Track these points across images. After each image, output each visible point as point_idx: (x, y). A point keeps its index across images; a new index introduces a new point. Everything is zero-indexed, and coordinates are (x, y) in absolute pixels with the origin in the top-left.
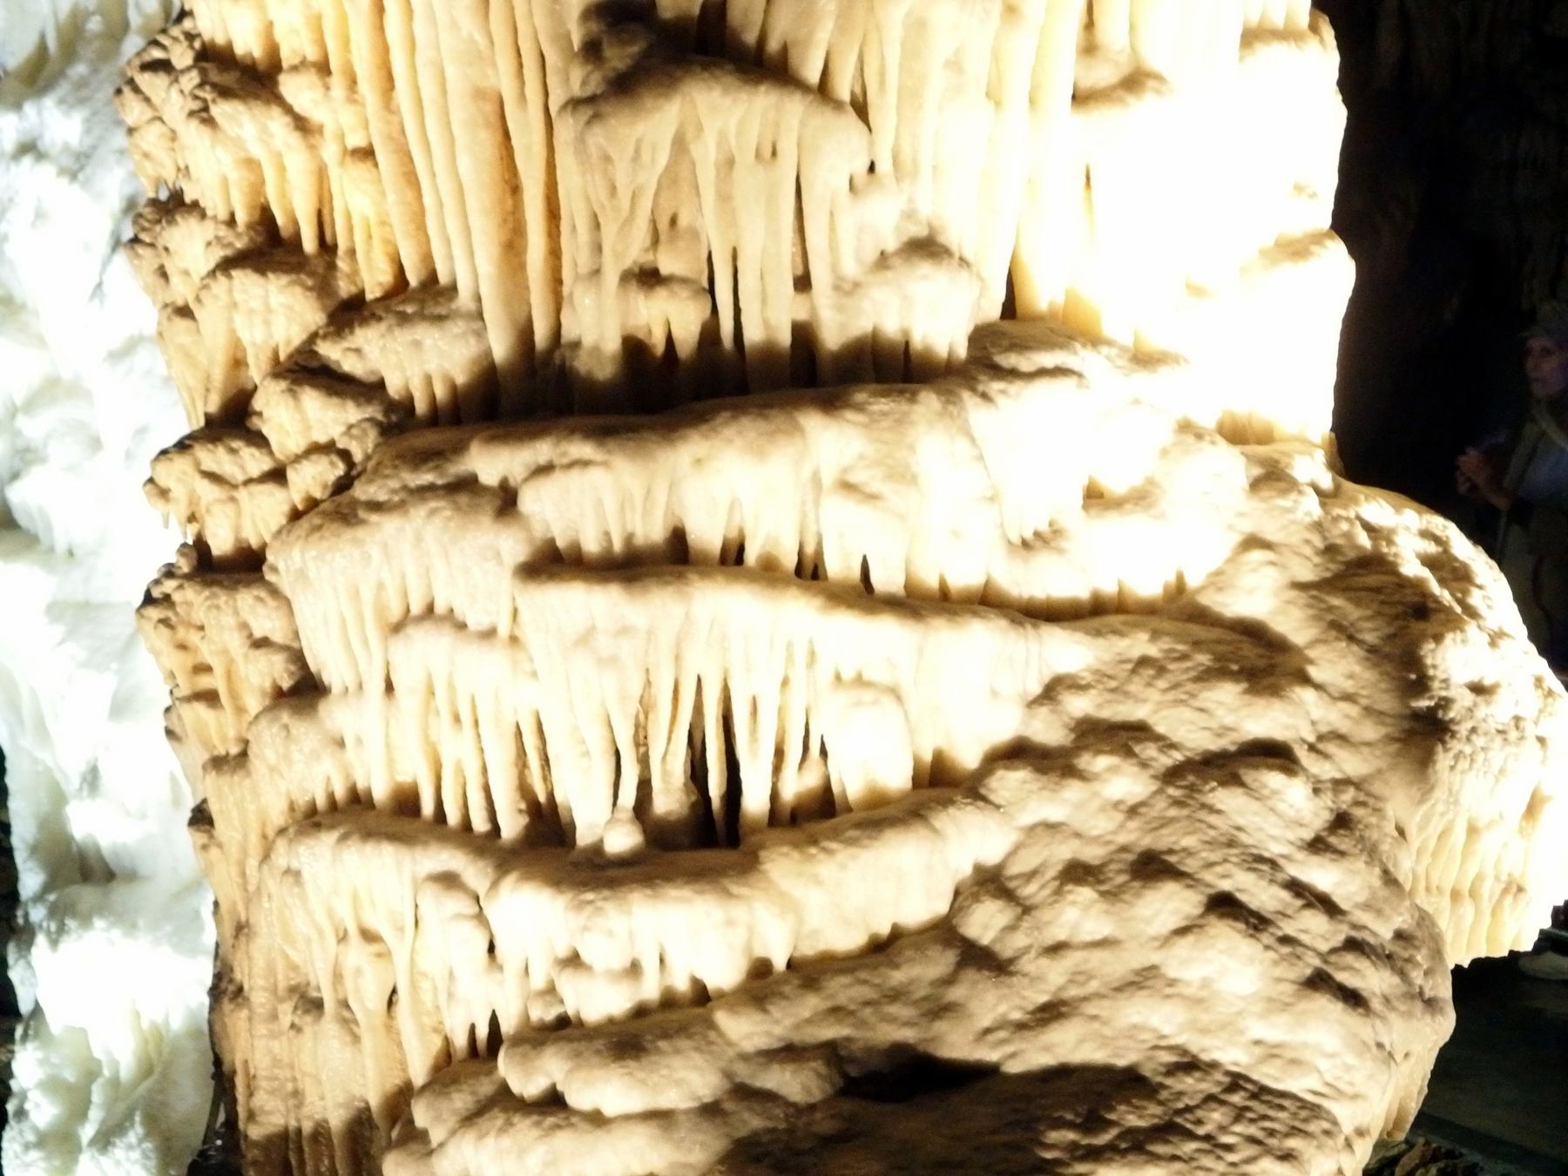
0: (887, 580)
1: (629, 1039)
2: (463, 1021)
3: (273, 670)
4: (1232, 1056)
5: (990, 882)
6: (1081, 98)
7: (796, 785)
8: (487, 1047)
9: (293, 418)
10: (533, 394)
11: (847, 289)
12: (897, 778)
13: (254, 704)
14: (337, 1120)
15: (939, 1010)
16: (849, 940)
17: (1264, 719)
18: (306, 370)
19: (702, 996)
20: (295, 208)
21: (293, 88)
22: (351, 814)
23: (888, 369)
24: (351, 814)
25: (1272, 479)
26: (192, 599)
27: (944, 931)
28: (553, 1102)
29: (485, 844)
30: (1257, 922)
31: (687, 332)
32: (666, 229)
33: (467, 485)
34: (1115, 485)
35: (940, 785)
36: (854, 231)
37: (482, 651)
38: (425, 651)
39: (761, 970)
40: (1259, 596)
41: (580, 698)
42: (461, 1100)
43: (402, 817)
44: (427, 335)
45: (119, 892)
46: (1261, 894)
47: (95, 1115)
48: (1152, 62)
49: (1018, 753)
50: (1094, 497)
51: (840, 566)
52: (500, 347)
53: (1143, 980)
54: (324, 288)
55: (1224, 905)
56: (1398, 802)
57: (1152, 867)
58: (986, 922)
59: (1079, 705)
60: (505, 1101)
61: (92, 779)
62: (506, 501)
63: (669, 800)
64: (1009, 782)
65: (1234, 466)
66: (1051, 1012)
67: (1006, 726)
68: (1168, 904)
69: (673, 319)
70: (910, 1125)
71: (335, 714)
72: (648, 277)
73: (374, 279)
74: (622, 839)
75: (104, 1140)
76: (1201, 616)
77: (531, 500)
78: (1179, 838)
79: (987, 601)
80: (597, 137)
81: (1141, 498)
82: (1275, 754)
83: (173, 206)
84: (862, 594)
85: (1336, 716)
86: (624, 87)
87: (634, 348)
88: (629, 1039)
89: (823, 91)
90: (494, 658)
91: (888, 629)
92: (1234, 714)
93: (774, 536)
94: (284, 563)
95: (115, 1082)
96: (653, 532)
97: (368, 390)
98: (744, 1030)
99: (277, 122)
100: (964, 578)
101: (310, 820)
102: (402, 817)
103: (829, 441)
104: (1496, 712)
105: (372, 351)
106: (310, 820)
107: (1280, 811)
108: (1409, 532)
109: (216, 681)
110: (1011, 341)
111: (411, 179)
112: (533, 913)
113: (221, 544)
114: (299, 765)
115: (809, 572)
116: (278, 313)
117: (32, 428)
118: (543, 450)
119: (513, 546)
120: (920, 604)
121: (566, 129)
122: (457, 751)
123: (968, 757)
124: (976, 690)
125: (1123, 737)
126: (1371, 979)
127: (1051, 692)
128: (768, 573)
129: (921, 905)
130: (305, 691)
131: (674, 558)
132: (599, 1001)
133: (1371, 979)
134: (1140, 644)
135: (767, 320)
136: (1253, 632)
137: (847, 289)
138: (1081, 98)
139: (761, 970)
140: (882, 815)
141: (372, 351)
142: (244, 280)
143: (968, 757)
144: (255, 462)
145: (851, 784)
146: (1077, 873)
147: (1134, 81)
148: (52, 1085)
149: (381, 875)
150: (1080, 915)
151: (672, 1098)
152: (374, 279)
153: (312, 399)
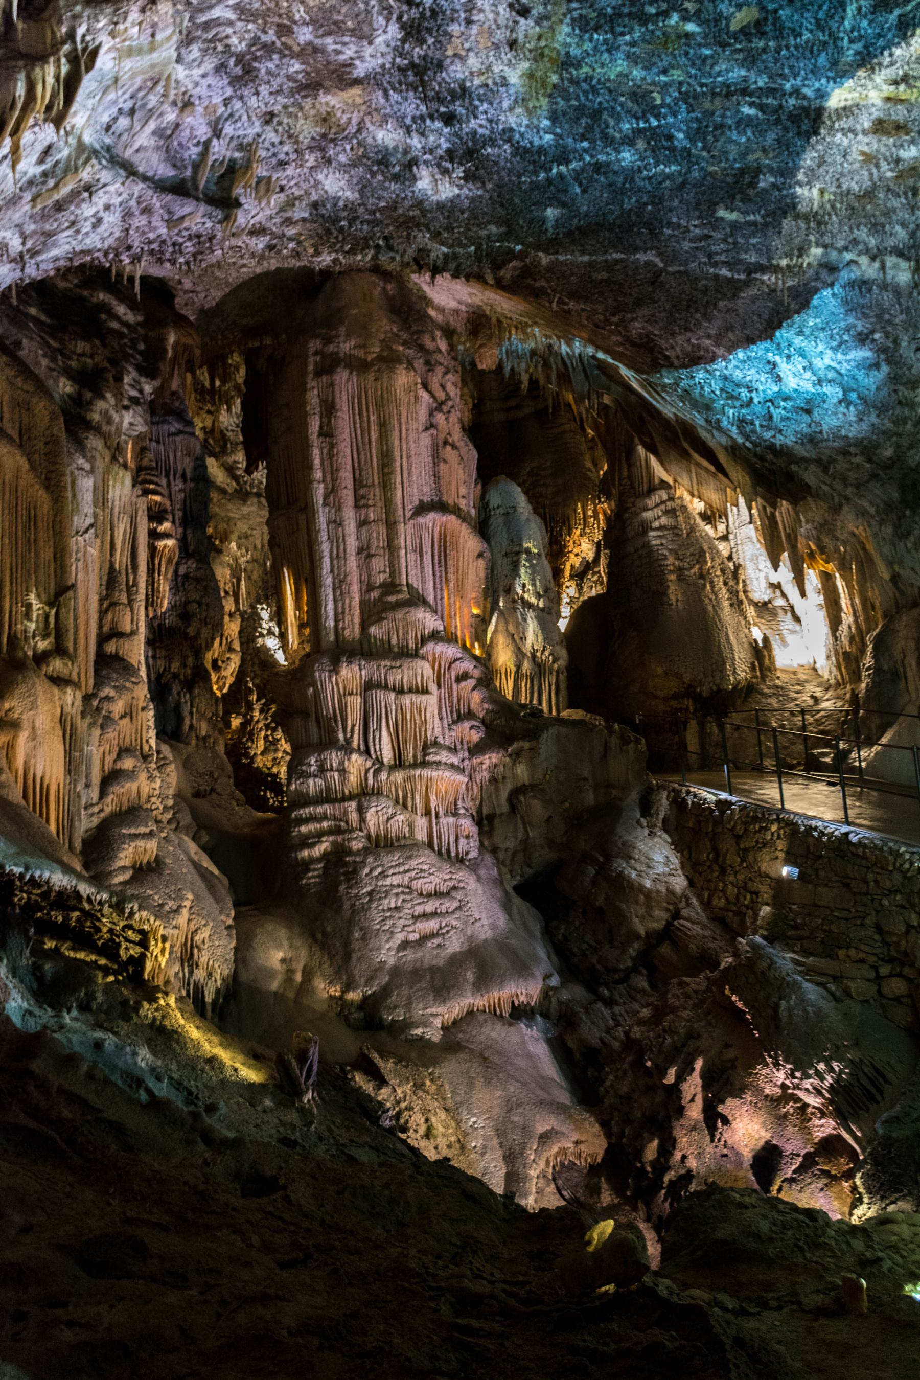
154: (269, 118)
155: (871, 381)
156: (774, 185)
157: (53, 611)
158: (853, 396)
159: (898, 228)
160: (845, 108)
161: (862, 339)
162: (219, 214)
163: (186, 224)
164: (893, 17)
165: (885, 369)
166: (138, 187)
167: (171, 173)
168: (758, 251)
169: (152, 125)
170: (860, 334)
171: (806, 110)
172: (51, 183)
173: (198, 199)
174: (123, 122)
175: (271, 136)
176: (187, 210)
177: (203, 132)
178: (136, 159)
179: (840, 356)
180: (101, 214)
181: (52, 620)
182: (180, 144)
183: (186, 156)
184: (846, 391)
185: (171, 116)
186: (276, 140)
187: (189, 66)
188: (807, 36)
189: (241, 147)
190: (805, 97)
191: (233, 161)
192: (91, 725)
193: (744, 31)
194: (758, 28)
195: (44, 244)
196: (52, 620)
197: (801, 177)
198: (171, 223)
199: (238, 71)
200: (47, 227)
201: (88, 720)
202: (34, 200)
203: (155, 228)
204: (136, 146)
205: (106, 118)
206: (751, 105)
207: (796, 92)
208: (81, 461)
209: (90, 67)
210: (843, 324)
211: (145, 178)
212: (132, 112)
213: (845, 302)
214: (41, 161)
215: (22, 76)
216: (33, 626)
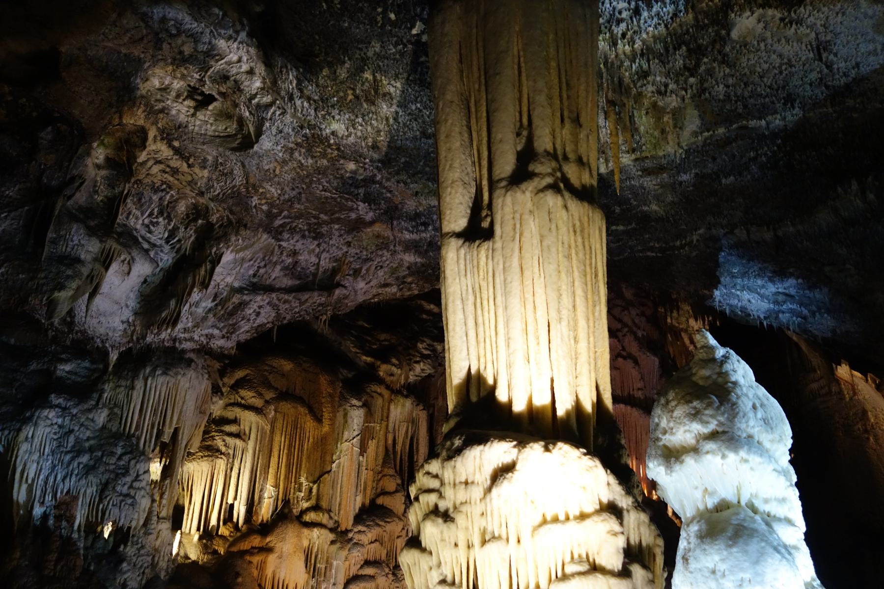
154: (349, 244)
157: (315, 486)
162: (326, 294)
163: (311, 301)
166: (274, 295)
167: (298, 282)
169: (279, 267)
172: (220, 308)
173: (313, 290)
174: (262, 271)
175: (352, 251)
176: (307, 296)
177: (314, 259)
178: (273, 283)
180: (258, 310)
181: (314, 491)
182: (303, 268)
183: (308, 271)
185: (290, 260)
186: (358, 251)
187: (288, 240)
189: (336, 261)
191: (334, 267)
192: (341, 548)
195: (234, 329)
196: (314, 491)
198: (302, 303)
199: (312, 234)
200: (231, 322)
201: (338, 545)
202: (214, 316)
203: (296, 307)
204: (273, 277)
205: (251, 272)
208: (355, 402)
209: (219, 262)
211: (280, 290)
212: (265, 266)
214: (213, 301)
215: (191, 275)
216: (302, 494)
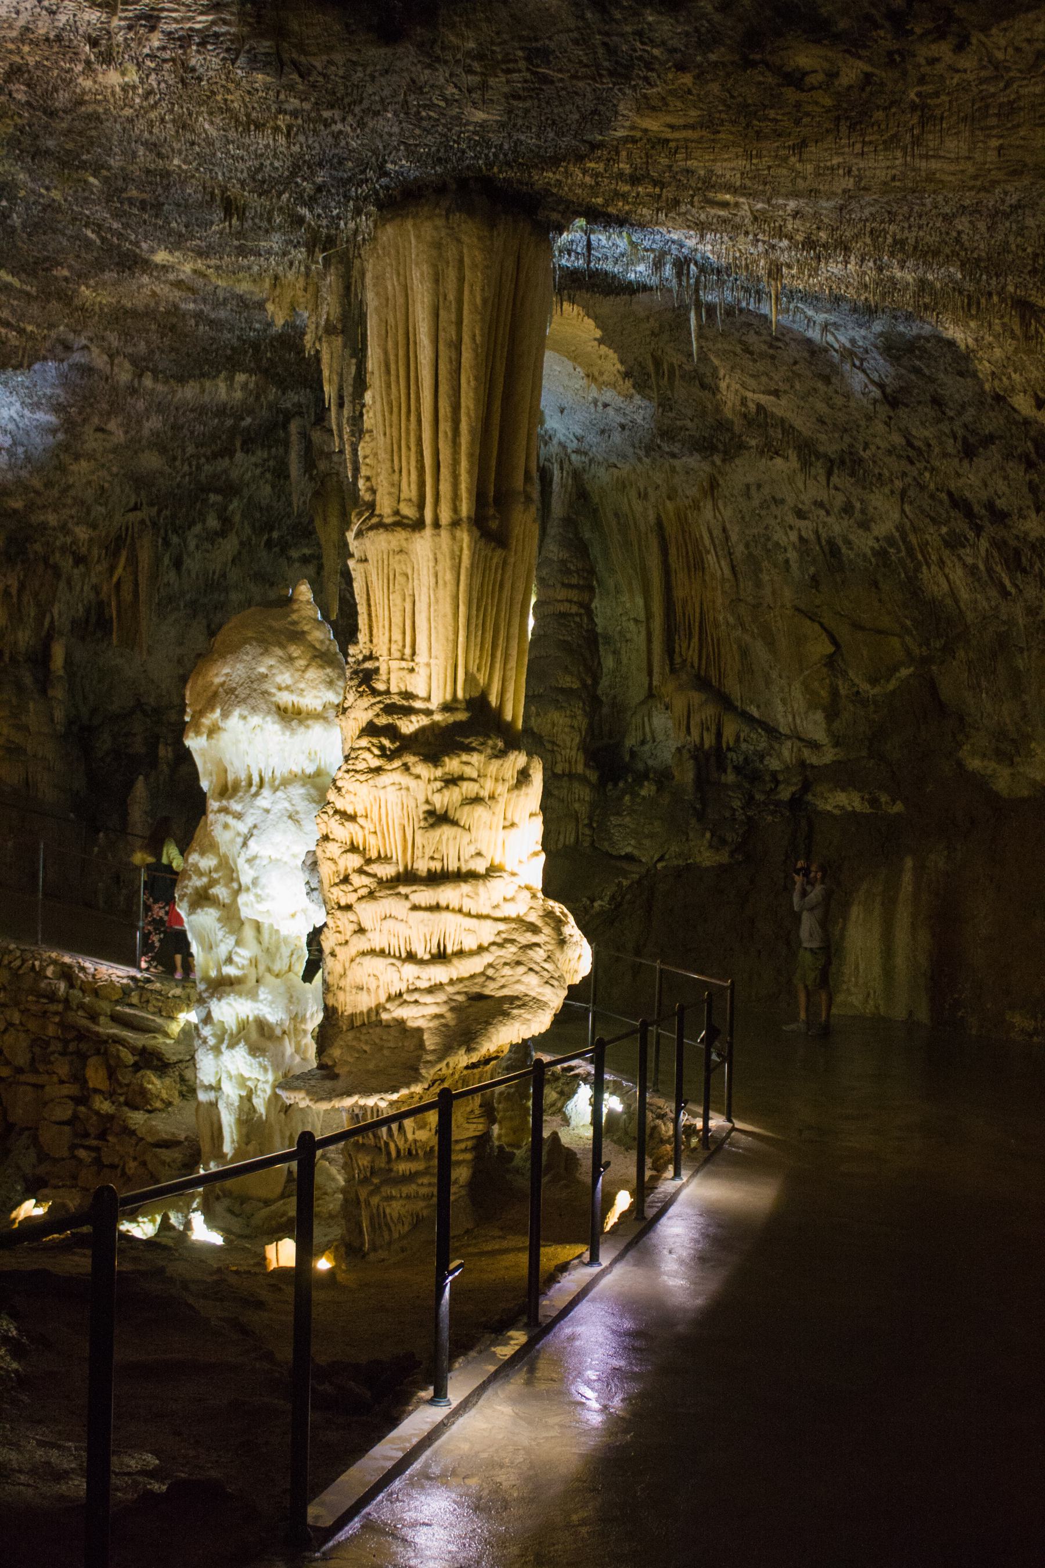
0: (473, 912)
1: (430, 990)
2: (394, 990)
3: (356, 928)
4: (533, 994)
5: (490, 965)
6: (504, 828)
7: (456, 948)
8: (401, 995)
9: (357, 880)
10: (408, 877)
11: (466, 861)
12: (474, 947)
13: (349, 933)
14: (365, 1010)
15: (483, 986)
16: (467, 975)
17: (535, 939)
18: (361, 871)
19: (441, 984)
20: (359, 841)
21: (359, 820)
22: (372, 952)
23: (471, 876)
24: (372, 952)
25: (534, 896)
26: (338, 913)
27: (483, 974)
28: (416, 1002)
29: (400, 958)
30: (537, 973)
31: (439, 868)
32: (437, 850)
33: (399, 894)
34: (509, 896)
35: (481, 949)
36: (469, 851)
37: (397, 923)
38: (390, 923)
39: (451, 980)
40: (533, 918)
41: (419, 932)
42: (397, 1002)
43: (382, 953)
44: (387, 866)
45: (237, 988)
46: (537, 968)
47: (226, 1042)
48: (516, 821)
49: (494, 944)
50: (505, 899)
51: (465, 910)
52: (401, 869)
53: (518, 981)
54: (364, 856)
55: (531, 969)
56: (558, 954)
57: (518, 963)
58: (490, 972)
59: (504, 936)
60: (405, 1001)
61: (229, 960)
62: (407, 897)
63: (434, 951)
64: (493, 948)
65: (527, 894)
66: (503, 987)
67: (492, 939)
68: (521, 969)
69: (436, 866)
70: (480, 1004)
71: (369, 935)
72: (432, 858)
73: (374, 855)
74: (427, 957)
75: (231, 1046)
76: (523, 921)
77: (411, 897)
78: (523, 959)
79: (487, 917)
80: (427, 834)
81: (512, 899)
82: (537, 945)
83: (326, 838)
84: (469, 915)
85: (547, 939)
86: (432, 826)
87: (429, 870)
88: (430, 990)
89: (463, 827)
90: (403, 924)
91: (474, 921)
92: (530, 938)
93: (455, 904)
94: (357, 907)
95: (231, 1034)
96: (434, 903)
97: (375, 876)
98: (450, 989)
99: (357, 827)
100: (485, 912)
101: (364, 954)
102: (382, 953)
103: (465, 888)
104: (574, 939)
105: (373, 869)
106: (364, 954)
107: (539, 954)
108: (558, 908)
109: (341, 929)
110: (493, 871)
111: (384, 837)
112: (410, 970)
113: (343, 903)
114: (360, 944)
115: (460, 911)
116: (356, 860)
117: (215, 875)
118: (414, 888)
119: (408, 905)
120: (479, 917)
121: (419, 833)
122: (394, 942)
123: (486, 944)
124: (487, 932)
125: (512, 941)
126: (555, 983)
127: (499, 933)
128: (453, 910)
129: (479, 969)
130: (361, 930)
131: (436, 908)
132: (424, 984)
133: (555, 983)
134: (513, 925)
135: (453, 866)
136: (532, 924)
137: (466, 861)
138: (504, 828)
139: (451, 980)
140: (472, 953)
141: (373, 869)
142: (349, 855)
143: (486, 944)
144: (351, 888)
145: (466, 947)
146: (506, 964)
147: (513, 825)
148: (214, 1035)
149: (378, 964)
150: (507, 971)
151: (439, 1000)
152: (374, 855)
153: (363, 877)
155: (39, 442)
156: (66, 279)
158: (20, 450)
159: (143, 343)
160: (164, 266)
161: (58, 408)
164: (236, 243)
165: (60, 436)
168: (13, 311)
170: (59, 404)
171: (136, 255)
179: (26, 412)
184: (15, 443)
188: (174, 225)
190: (139, 247)
193: (131, 201)
194: (143, 206)
197: (92, 282)
206: (93, 231)
207: (137, 244)
210: (48, 391)
213: (64, 376)
